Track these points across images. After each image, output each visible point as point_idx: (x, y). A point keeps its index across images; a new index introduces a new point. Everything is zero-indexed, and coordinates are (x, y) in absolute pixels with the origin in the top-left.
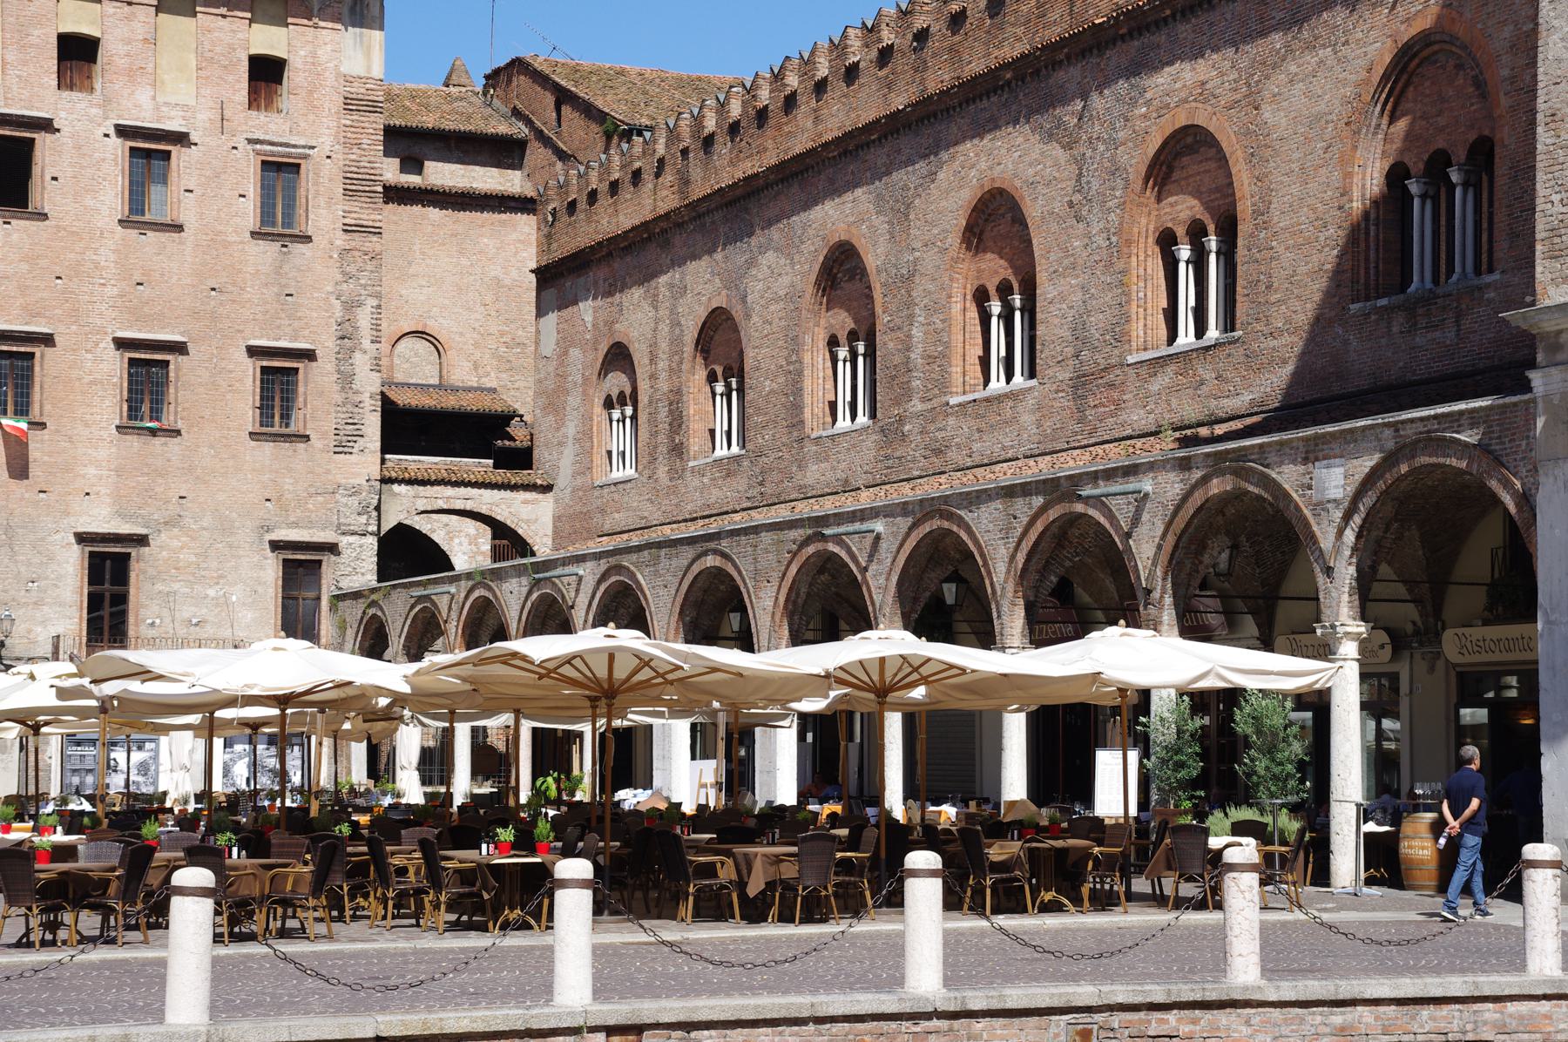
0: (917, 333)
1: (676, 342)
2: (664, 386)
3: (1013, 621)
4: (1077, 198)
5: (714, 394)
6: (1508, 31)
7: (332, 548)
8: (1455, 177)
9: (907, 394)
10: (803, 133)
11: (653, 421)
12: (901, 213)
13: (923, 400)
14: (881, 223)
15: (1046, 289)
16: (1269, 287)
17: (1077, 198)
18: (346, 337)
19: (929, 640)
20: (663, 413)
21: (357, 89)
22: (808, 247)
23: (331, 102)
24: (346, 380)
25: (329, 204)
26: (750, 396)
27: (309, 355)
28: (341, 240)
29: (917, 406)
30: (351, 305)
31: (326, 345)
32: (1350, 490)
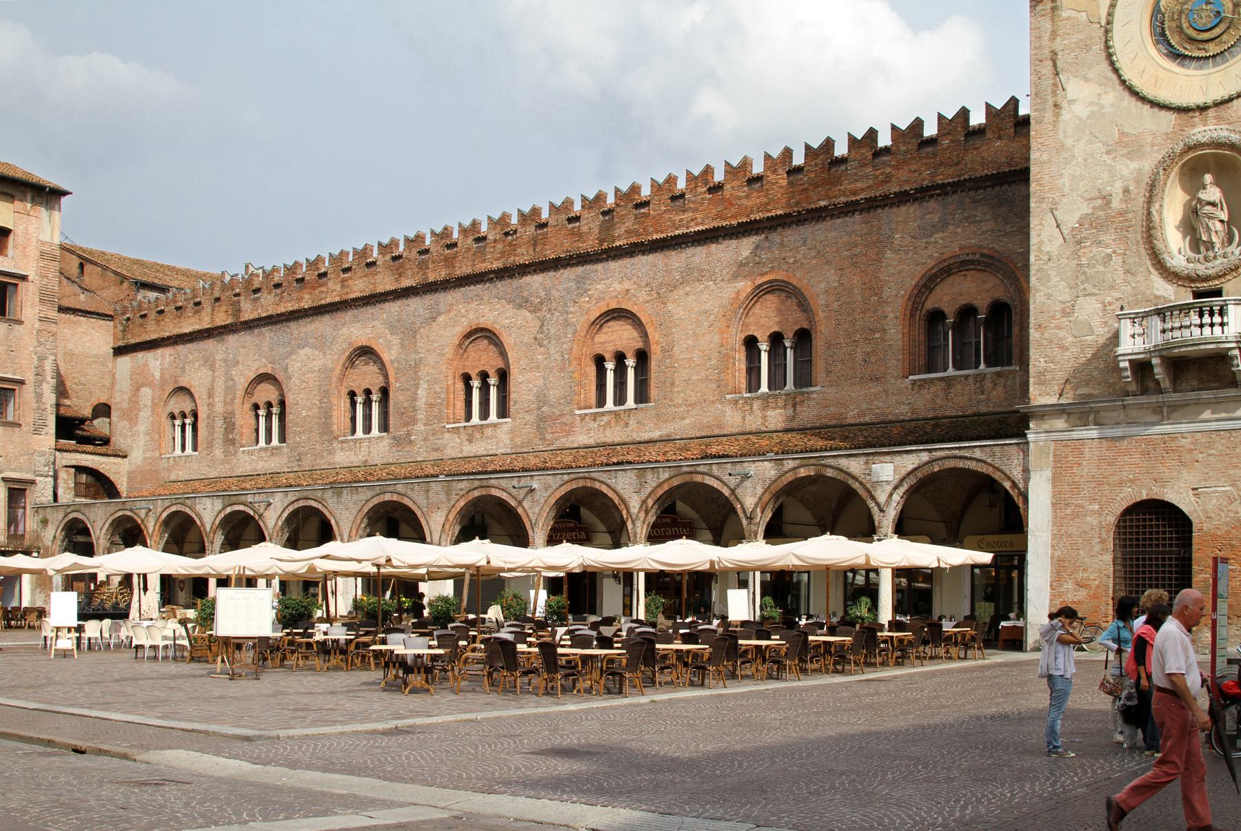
0: (421, 393)
1: (230, 389)
2: (219, 408)
3: (539, 534)
4: (539, 336)
5: (257, 416)
6: (823, 285)
7: (33, 482)
8: (788, 344)
9: (414, 421)
10: (332, 292)
11: (211, 427)
12: (410, 334)
13: (425, 425)
14: (395, 340)
15: (517, 379)
16: (673, 384)
17: (539, 336)
18: (39, 374)
19: (493, 541)
20: (219, 423)
21: (47, 248)
22: (337, 347)
23: (34, 253)
24: (39, 396)
25: (32, 305)
26: (289, 418)
27: (22, 382)
28: (37, 325)
29: (420, 427)
30: (42, 359)
31: (30, 377)
32: (898, 477)
